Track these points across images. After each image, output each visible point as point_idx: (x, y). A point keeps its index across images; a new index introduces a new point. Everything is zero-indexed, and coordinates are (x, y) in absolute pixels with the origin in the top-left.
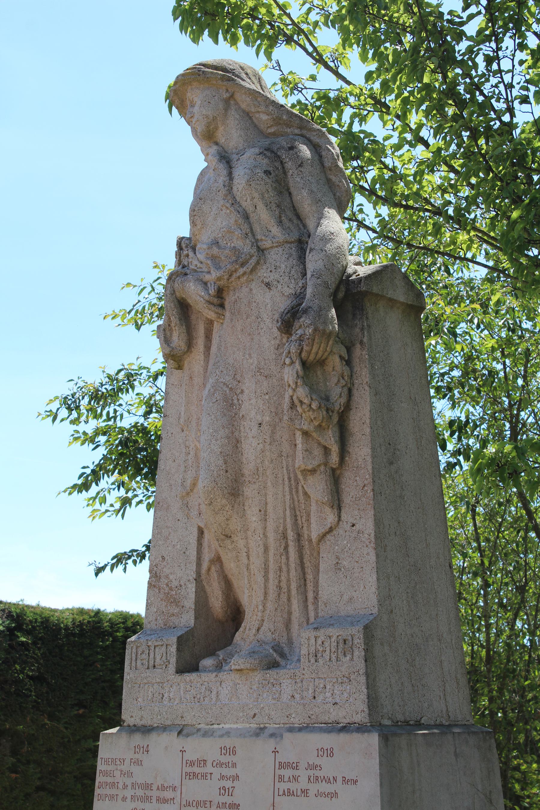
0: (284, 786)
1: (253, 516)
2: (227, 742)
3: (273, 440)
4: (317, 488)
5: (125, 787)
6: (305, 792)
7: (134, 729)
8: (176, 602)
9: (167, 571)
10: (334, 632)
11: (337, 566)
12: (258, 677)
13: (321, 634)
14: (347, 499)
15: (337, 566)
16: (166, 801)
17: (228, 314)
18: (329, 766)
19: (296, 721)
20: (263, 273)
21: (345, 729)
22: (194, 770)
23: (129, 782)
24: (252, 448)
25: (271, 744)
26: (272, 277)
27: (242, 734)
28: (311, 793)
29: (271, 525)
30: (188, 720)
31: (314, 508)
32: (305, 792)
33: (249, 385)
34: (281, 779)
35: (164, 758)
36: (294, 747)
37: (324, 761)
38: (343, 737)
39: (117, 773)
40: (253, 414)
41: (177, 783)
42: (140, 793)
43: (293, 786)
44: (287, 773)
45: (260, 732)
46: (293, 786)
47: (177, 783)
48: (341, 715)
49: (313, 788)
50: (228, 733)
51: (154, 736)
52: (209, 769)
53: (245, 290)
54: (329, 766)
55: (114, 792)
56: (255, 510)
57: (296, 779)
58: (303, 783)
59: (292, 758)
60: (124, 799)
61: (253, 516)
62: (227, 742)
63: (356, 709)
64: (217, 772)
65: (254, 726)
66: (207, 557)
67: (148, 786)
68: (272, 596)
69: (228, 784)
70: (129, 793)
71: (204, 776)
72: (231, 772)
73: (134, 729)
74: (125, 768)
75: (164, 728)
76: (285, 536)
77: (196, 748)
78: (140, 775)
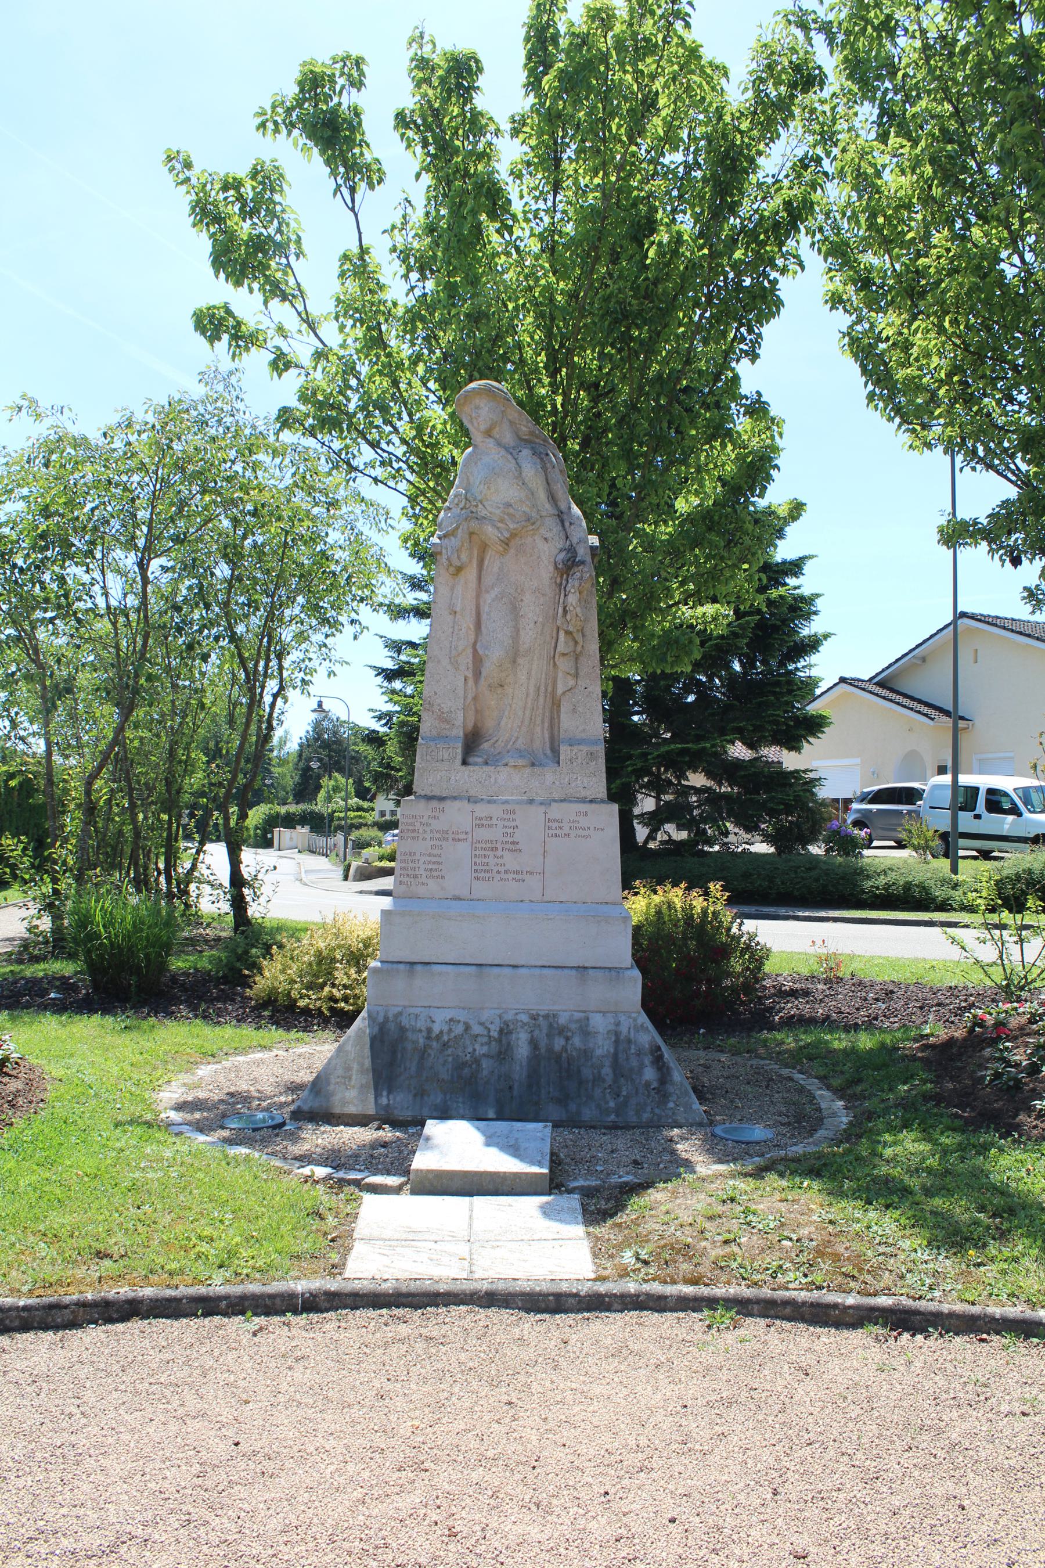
0: (551, 832)
1: (522, 677)
2: (509, 807)
3: (542, 633)
4: (564, 665)
5: (425, 832)
6: (568, 835)
7: (429, 798)
8: (448, 722)
9: (438, 701)
10: (585, 748)
11: (574, 710)
12: (528, 770)
13: (575, 749)
14: (581, 673)
15: (574, 710)
16: (459, 840)
17: (512, 551)
18: (583, 822)
19: (556, 796)
20: (542, 531)
21: (591, 801)
22: (481, 823)
23: (428, 829)
24: (528, 636)
25: (542, 809)
26: (548, 535)
27: (519, 802)
28: (572, 835)
29: (533, 681)
30: (472, 793)
31: (560, 675)
32: (568, 835)
33: (528, 598)
34: (550, 828)
35: (457, 815)
36: (556, 811)
37: (581, 818)
38: (593, 805)
39: (418, 824)
40: (530, 615)
41: (469, 830)
42: (438, 835)
43: (558, 832)
44: (554, 825)
45: (531, 802)
46: (558, 832)
47: (469, 830)
48: (589, 794)
49: (573, 833)
50: (506, 802)
51: (448, 802)
52: (494, 822)
53: (529, 540)
54: (583, 822)
55: (415, 835)
56: (525, 672)
57: (561, 828)
58: (566, 830)
59: (558, 816)
60: (424, 839)
61: (522, 677)
62: (509, 807)
63: (602, 792)
64: (500, 824)
65: (525, 798)
66: (470, 696)
67: (444, 832)
68: (526, 722)
69: (510, 831)
70: (428, 836)
71: (491, 826)
72: (514, 824)
73: (429, 798)
74: (425, 820)
75: (455, 798)
76: (538, 689)
77: (481, 810)
78: (436, 825)
